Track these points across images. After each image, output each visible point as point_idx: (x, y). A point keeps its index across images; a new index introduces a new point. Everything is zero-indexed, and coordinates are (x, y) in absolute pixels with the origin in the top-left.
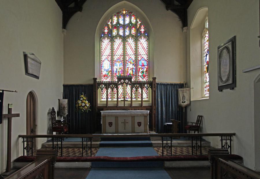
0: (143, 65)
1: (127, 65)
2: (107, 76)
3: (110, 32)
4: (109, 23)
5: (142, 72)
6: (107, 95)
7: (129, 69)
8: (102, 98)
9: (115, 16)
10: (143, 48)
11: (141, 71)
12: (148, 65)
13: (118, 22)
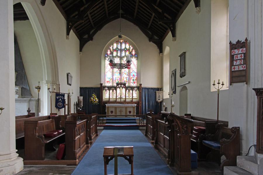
0: (134, 76)
1: (123, 75)
2: (109, 82)
3: (112, 53)
4: (111, 48)
5: (133, 80)
6: (109, 94)
7: (124, 78)
8: (106, 96)
9: (115, 43)
10: (134, 65)
11: (132, 79)
12: (137, 75)
13: (117, 48)
